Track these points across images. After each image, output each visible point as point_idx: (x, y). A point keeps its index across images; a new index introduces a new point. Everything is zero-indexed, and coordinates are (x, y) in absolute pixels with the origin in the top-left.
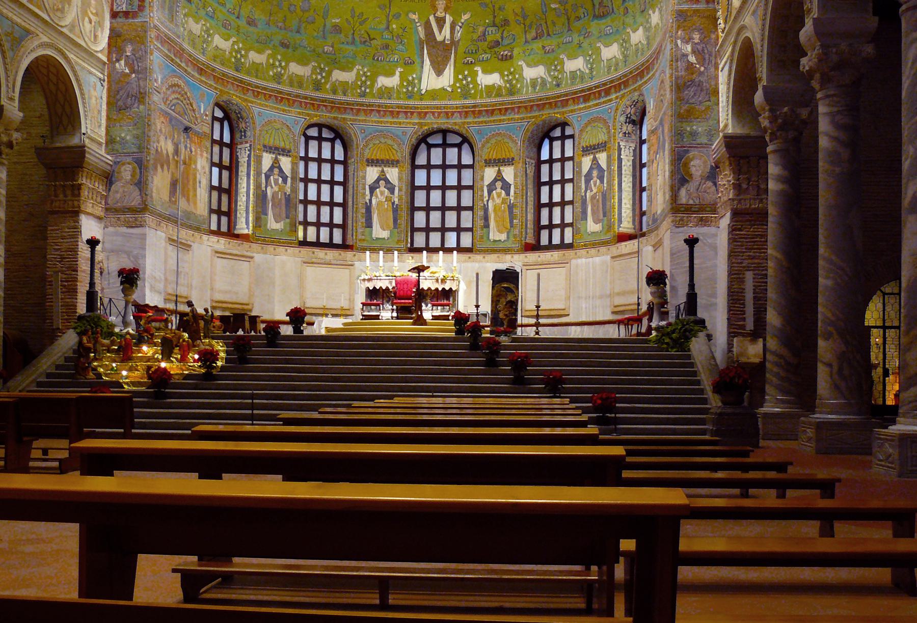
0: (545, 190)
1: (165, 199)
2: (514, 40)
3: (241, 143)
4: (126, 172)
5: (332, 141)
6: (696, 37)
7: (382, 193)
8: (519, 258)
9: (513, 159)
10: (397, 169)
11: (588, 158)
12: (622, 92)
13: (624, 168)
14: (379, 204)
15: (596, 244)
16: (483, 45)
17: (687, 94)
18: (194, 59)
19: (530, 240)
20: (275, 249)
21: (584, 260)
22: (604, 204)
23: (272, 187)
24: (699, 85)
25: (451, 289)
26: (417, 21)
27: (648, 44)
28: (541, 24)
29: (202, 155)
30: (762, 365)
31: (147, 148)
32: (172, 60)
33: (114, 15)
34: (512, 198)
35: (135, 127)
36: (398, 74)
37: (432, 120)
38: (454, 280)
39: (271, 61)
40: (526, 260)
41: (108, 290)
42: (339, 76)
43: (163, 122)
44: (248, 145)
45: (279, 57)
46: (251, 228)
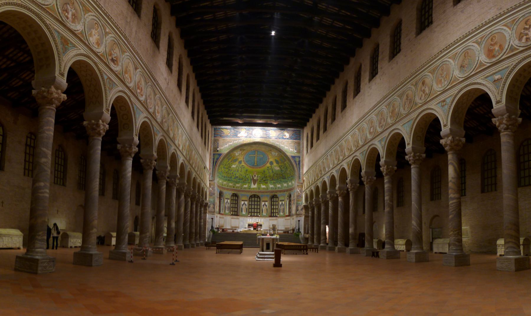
4: (212, 206)
14: (244, 208)
15: (282, 217)
16: (263, 180)
19: (270, 215)
30: (308, 238)
33: (210, 181)
42: (237, 185)
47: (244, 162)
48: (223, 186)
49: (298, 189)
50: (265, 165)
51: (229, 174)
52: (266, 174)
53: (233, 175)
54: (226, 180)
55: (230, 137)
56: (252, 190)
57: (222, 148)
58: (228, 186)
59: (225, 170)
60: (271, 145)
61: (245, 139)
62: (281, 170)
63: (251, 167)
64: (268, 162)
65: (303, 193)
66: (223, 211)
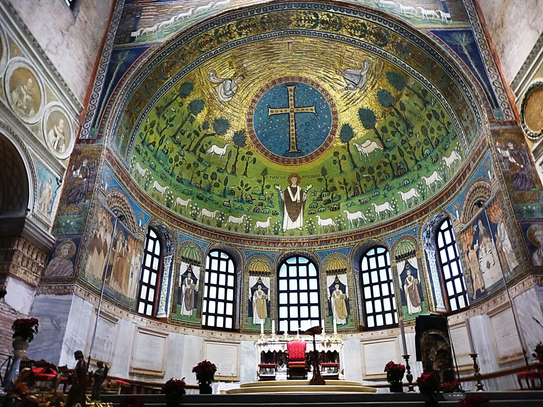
1: (98, 276)
2: (340, 198)
3: (167, 255)
5: (227, 261)
6: (511, 146)
7: (260, 294)
9: (346, 269)
12: (423, 217)
13: (431, 267)
16: (321, 203)
18: (139, 190)
19: (362, 324)
20: (185, 330)
21: (409, 334)
23: (186, 286)
24: (523, 177)
25: (335, 351)
27: (445, 179)
29: (136, 256)
31: (86, 231)
33: (78, 141)
34: (347, 295)
38: (337, 343)
39: (191, 206)
40: (362, 337)
43: (104, 218)
44: (171, 256)
45: (196, 204)
46: (168, 313)
47: (252, 138)
48: (171, 211)
49: (506, 148)
50: (327, 145)
52: (331, 181)
53: (217, 181)
54: (186, 194)
56: (287, 236)
59: (178, 153)
62: (385, 148)
63: (277, 160)
64: (333, 133)
65: (533, 164)
66: (166, 310)
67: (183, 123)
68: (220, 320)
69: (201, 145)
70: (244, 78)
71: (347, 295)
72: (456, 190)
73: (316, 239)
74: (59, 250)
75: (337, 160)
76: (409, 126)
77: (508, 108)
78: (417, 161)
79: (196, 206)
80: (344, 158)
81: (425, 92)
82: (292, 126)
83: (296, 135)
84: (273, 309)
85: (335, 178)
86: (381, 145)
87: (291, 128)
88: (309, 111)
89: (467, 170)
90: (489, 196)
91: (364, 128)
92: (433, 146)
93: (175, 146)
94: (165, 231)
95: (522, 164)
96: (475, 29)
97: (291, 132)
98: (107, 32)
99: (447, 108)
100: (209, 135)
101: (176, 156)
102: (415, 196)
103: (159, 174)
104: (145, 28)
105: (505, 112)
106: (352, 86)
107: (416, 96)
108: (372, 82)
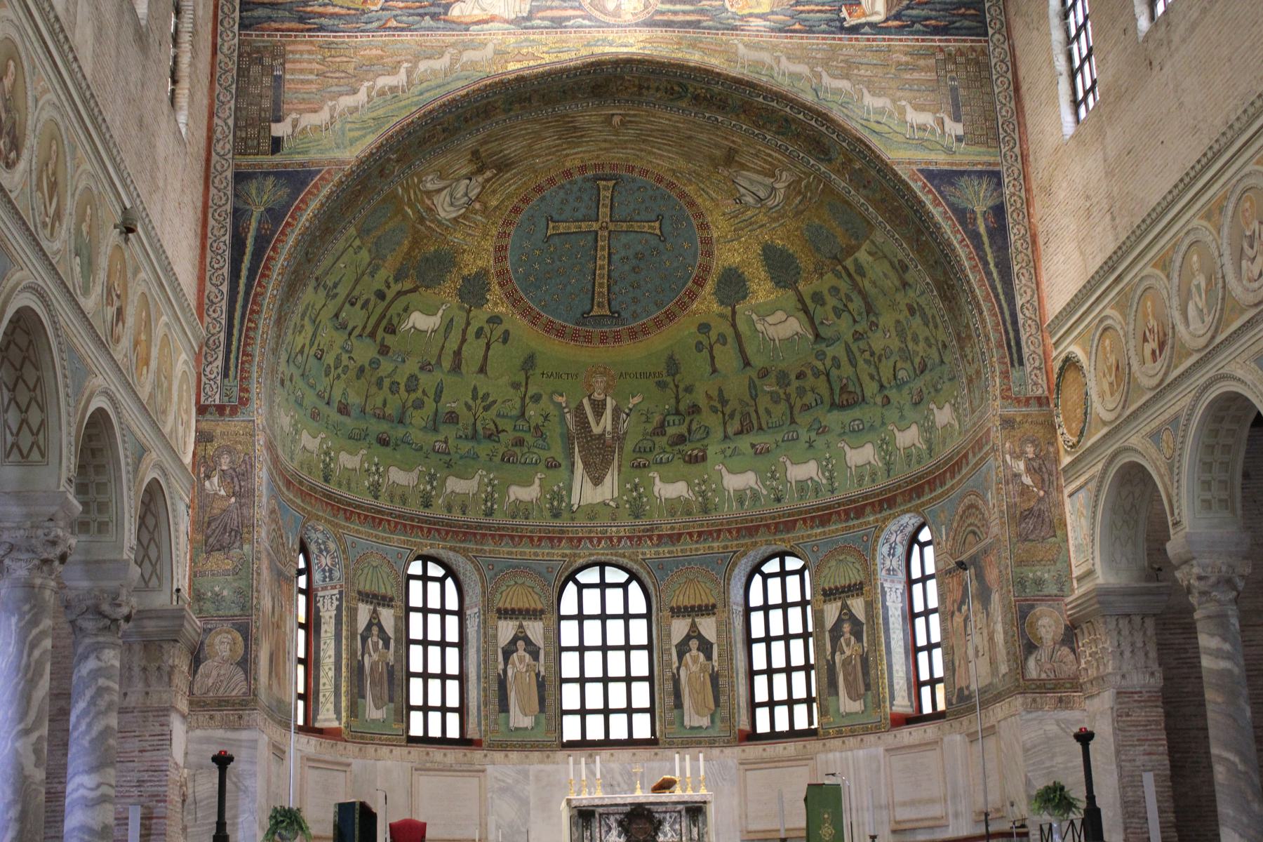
0: (759, 650)
3: (324, 589)
4: (223, 644)
5: (442, 581)
6: (1030, 450)
7: (521, 660)
8: (733, 753)
9: (714, 606)
10: (541, 624)
11: (834, 605)
12: (885, 514)
13: (891, 620)
16: (662, 441)
17: (1024, 528)
19: (744, 725)
21: (838, 754)
22: (866, 673)
23: (370, 656)
26: (564, 405)
27: (930, 449)
28: (748, 413)
32: (272, 474)
33: (202, 410)
34: (716, 664)
35: (236, 577)
36: (537, 481)
37: (588, 548)
39: (366, 465)
40: (744, 756)
41: (194, 829)
42: (455, 485)
44: (336, 591)
45: (376, 460)
46: (344, 720)
47: (501, 285)
48: (332, 488)
50: (683, 306)
51: (387, 383)
52: (689, 390)
53: (419, 393)
54: (357, 438)
55: (383, 28)
56: (581, 521)
57: (309, 120)
58: (376, 487)
60: (738, 82)
61: (512, 39)
62: (817, 336)
63: (561, 333)
64: (700, 282)
65: (1060, 490)
67: (357, 282)
68: (435, 718)
69: (388, 316)
70: (500, 170)
71: (716, 664)
72: (943, 484)
73: (648, 530)
74: (212, 645)
75: (706, 342)
76: (869, 309)
77: (1040, 369)
78: (882, 387)
79: (376, 465)
80: (722, 339)
81: (905, 268)
82: (603, 258)
83: (609, 277)
84: (550, 691)
85: (697, 384)
86: (811, 331)
87: (599, 262)
88: (645, 230)
89: (964, 461)
90: (987, 534)
91: (770, 285)
92: (914, 368)
93: (336, 334)
94: (320, 536)
95: (1042, 488)
96: (1007, 170)
97: (598, 272)
98: (211, 115)
99: (943, 316)
100: (406, 292)
101: (338, 355)
102: (873, 462)
103: (309, 412)
104: (301, 112)
105: (1033, 376)
106: (750, 199)
107: (886, 266)
108: (797, 206)
